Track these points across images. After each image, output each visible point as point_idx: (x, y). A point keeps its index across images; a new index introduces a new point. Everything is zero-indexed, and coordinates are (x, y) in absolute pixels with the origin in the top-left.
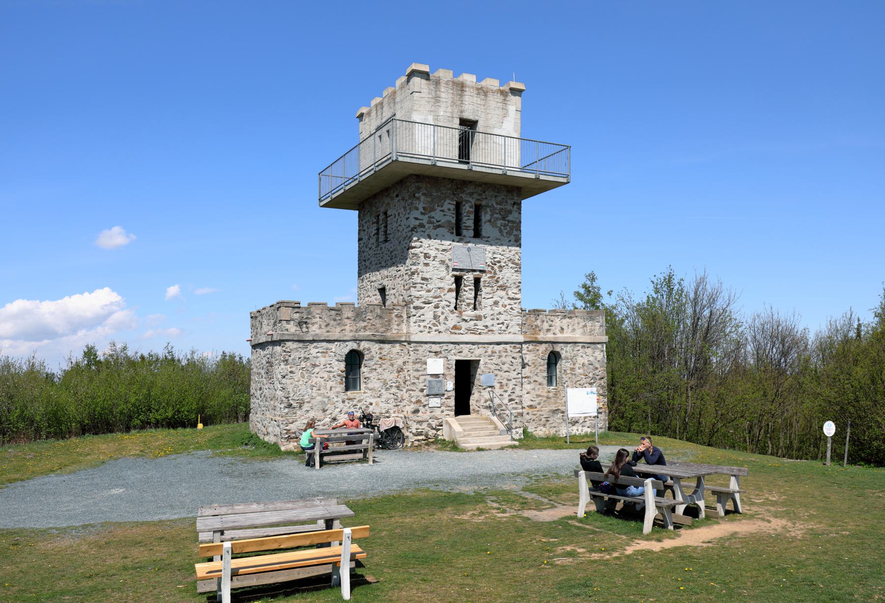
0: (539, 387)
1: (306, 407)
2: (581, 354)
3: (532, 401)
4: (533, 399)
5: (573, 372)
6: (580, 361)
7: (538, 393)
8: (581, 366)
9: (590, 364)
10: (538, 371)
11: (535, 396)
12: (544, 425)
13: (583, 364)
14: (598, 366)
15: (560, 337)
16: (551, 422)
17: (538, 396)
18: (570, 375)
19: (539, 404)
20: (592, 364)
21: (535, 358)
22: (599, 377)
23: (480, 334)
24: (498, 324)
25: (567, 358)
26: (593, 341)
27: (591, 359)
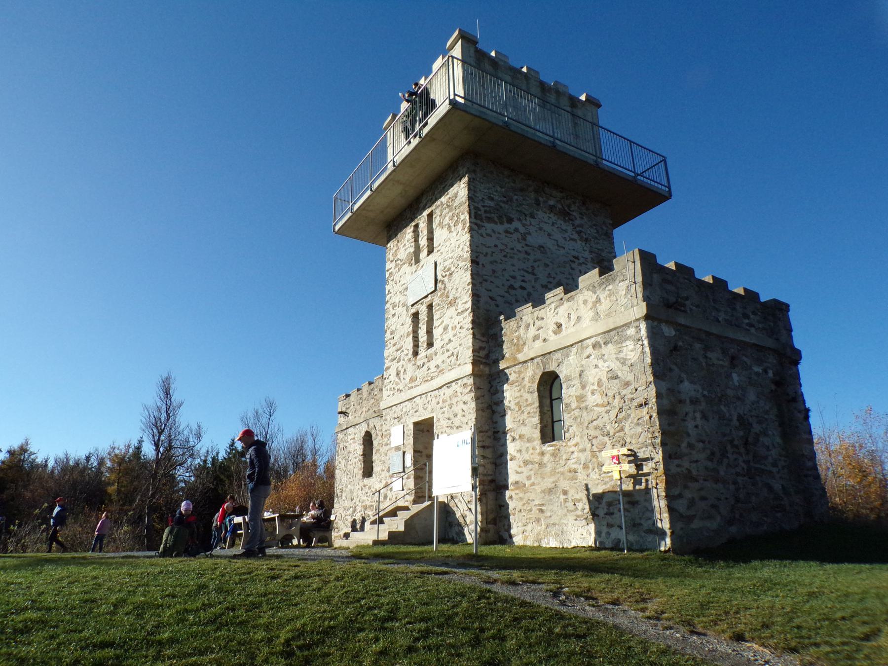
0: (528, 445)
1: (344, 494)
2: (595, 362)
3: (517, 473)
4: (519, 470)
5: (583, 405)
6: (592, 376)
7: (527, 457)
8: (596, 387)
9: (612, 378)
10: (525, 416)
11: (522, 464)
12: (538, 520)
13: (600, 381)
14: (630, 377)
15: (555, 342)
16: (549, 514)
17: (526, 463)
18: (577, 413)
19: (529, 478)
20: (616, 377)
21: (518, 394)
22: (635, 403)
23: (432, 379)
24: (449, 357)
25: (569, 379)
26: (612, 327)
27: (614, 365)
